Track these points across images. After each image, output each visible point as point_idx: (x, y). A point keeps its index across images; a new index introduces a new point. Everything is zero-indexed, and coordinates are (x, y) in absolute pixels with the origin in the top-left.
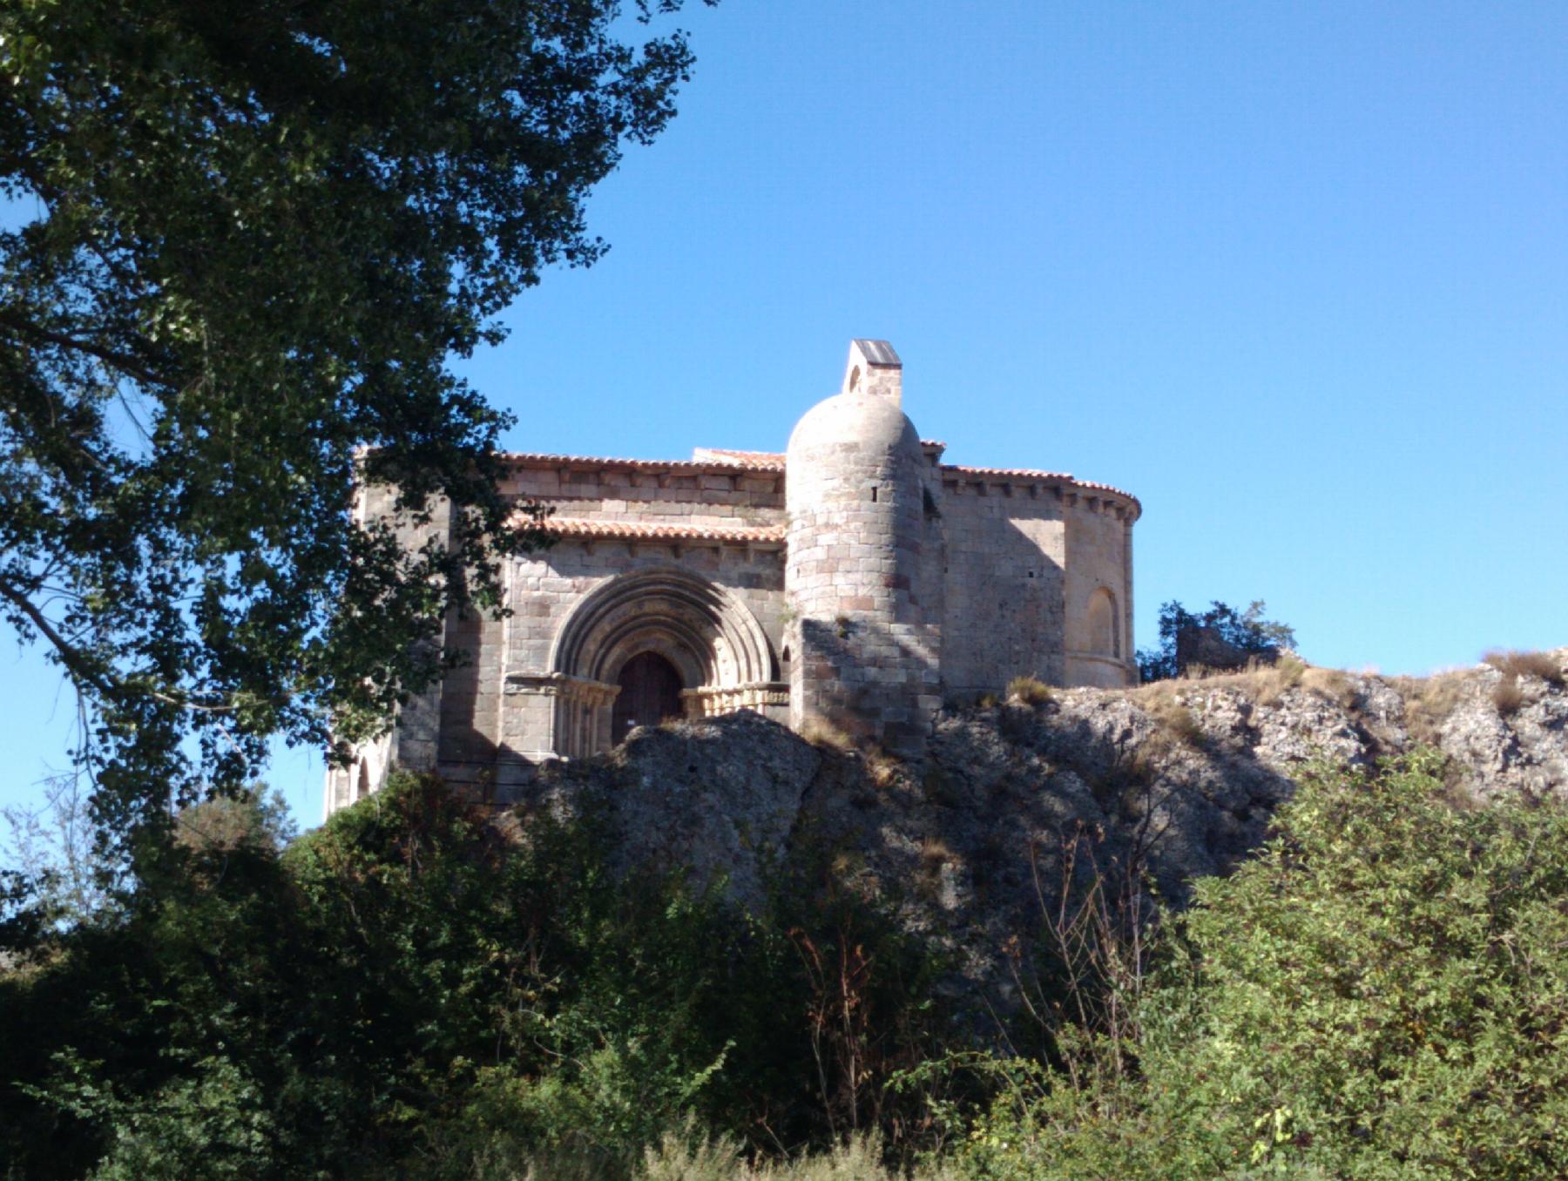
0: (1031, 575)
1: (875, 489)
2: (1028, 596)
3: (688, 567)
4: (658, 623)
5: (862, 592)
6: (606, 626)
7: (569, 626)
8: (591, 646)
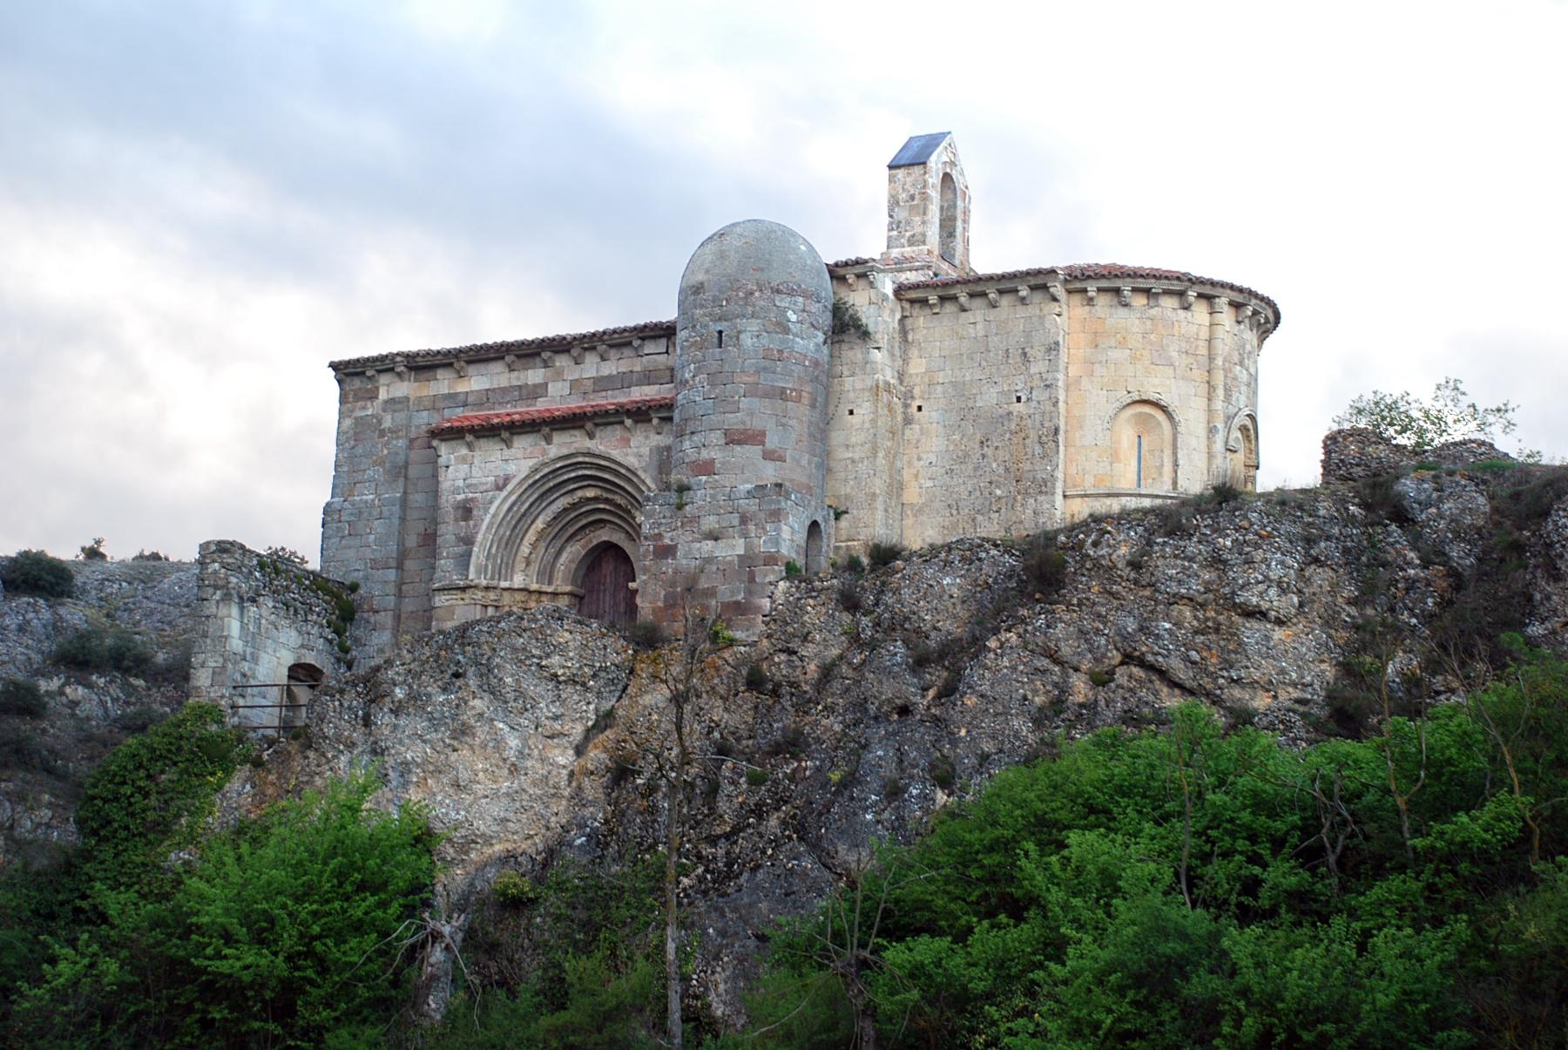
0: (1019, 399)
1: (720, 332)
2: (1013, 427)
6: (540, 524)
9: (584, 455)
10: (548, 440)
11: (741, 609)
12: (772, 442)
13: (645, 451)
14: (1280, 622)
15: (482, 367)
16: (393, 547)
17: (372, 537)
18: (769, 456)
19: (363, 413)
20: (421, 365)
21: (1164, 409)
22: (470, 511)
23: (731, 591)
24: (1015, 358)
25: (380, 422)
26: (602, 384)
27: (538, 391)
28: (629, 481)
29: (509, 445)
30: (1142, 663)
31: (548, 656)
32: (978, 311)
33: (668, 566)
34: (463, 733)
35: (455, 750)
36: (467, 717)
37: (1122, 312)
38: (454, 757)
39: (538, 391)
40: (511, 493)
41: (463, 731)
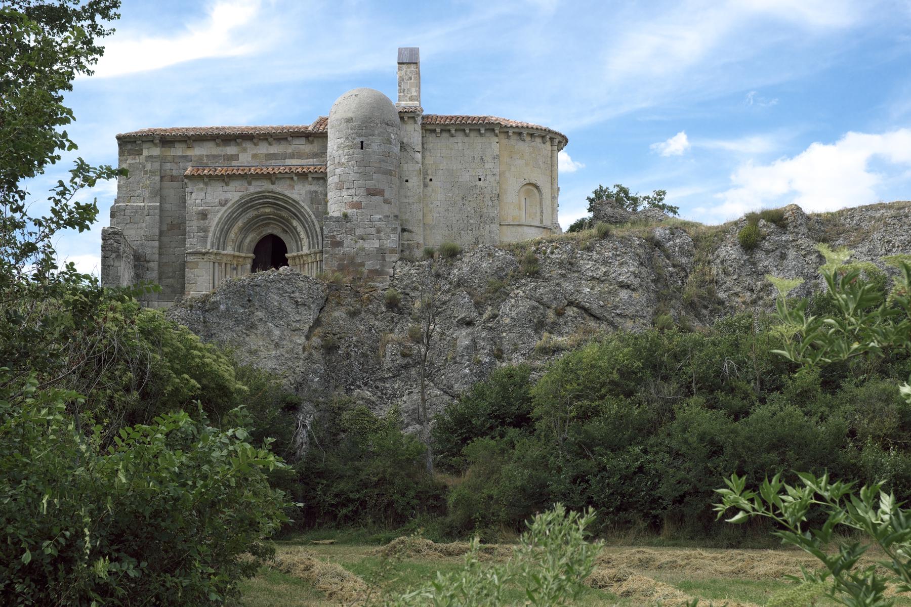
0: (480, 180)
1: (362, 142)
2: (478, 192)
4: (270, 219)
5: (355, 199)
6: (240, 223)
7: (217, 224)
8: (232, 235)
9: (269, 192)
10: (250, 184)
11: (378, 273)
12: (387, 195)
14: (634, 290)
16: (157, 231)
17: (144, 225)
18: (386, 202)
19: (133, 161)
21: (537, 187)
22: (206, 215)
23: (370, 265)
24: (478, 160)
25: (144, 167)
27: (235, 157)
28: (293, 206)
30: (578, 306)
31: (293, 292)
32: (460, 138)
33: (339, 251)
34: (252, 327)
35: (248, 335)
36: (254, 319)
37: (521, 143)
38: (247, 339)
39: (235, 157)
40: (229, 208)
41: (253, 326)
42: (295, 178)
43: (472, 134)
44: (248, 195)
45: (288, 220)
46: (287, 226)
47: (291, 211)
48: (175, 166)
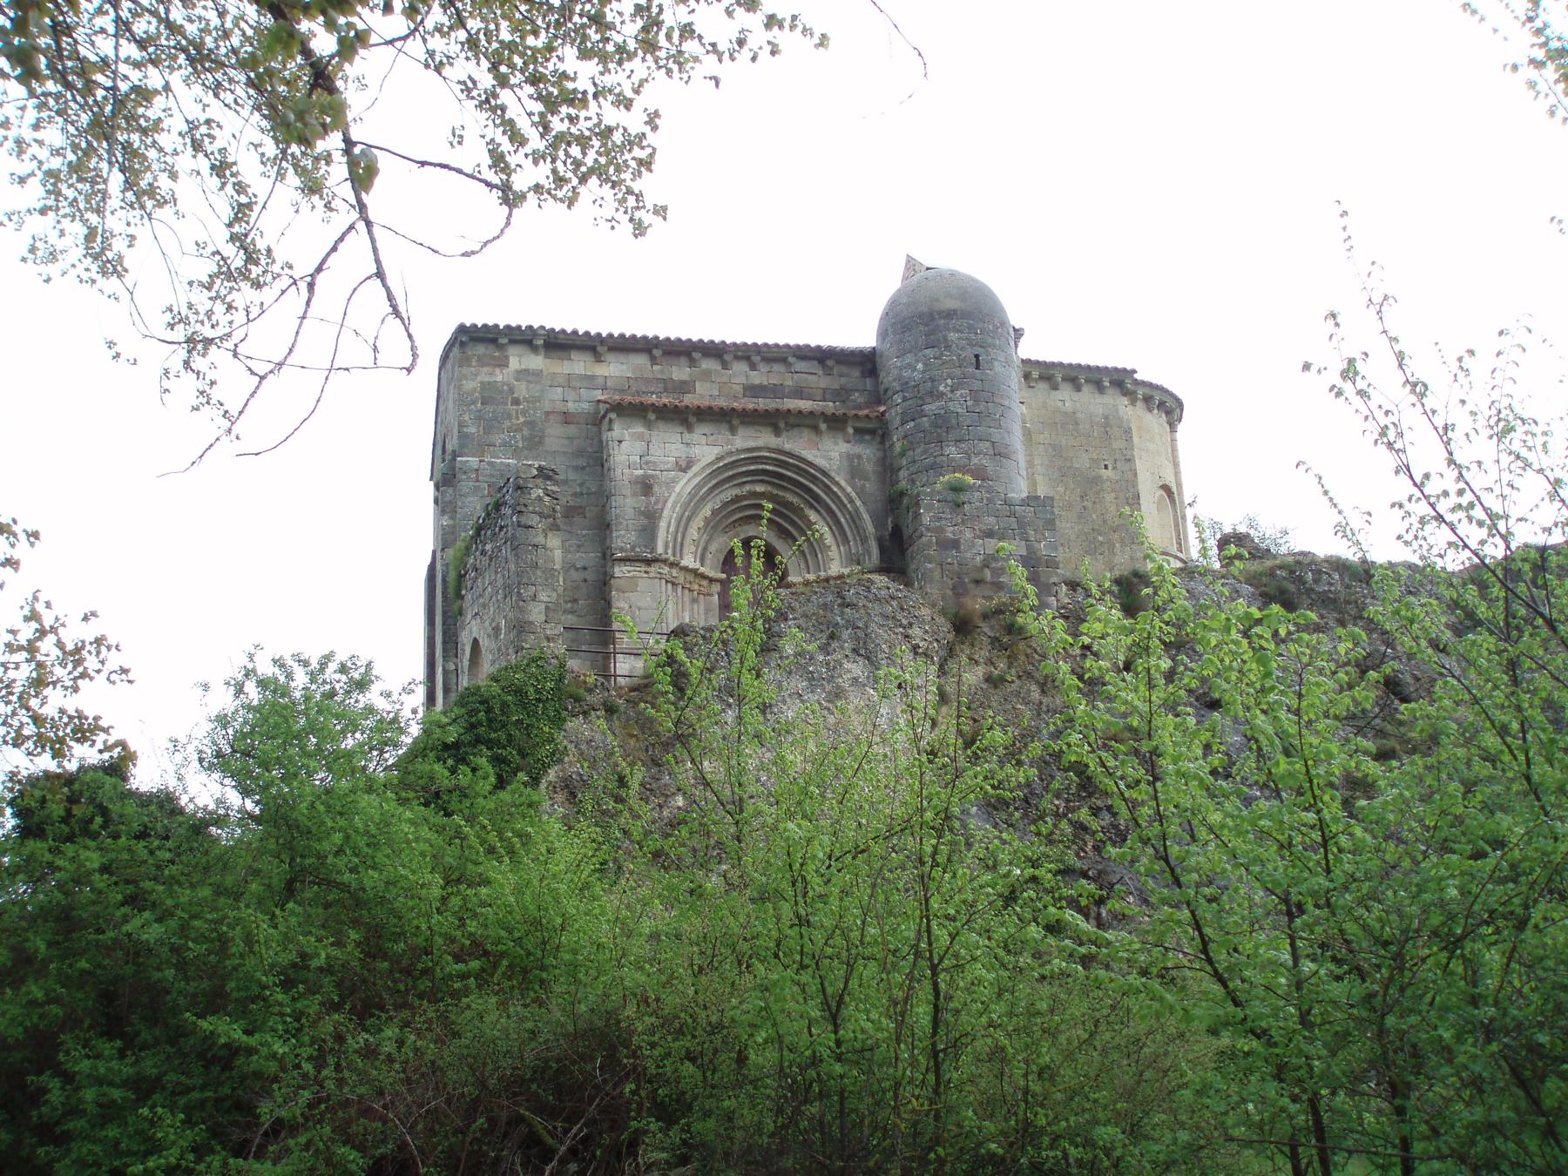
0: (1106, 467)
1: (977, 356)
3: (787, 447)
6: (707, 511)
8: (693, 533)
13: (835, 455)
15: (622, 357)
20: (557, 343)
25: (511, 391)
26: (753, 391)
29: (690, 429)
33: (951, 556)
34: (838, 696)
39: (684, 387)
42: (823, 426)
43: (1086, 389)
44: (730, 453)
45: (798, 511)
46: (793, 523)
47: (809, 491)
48: (571, 395)
